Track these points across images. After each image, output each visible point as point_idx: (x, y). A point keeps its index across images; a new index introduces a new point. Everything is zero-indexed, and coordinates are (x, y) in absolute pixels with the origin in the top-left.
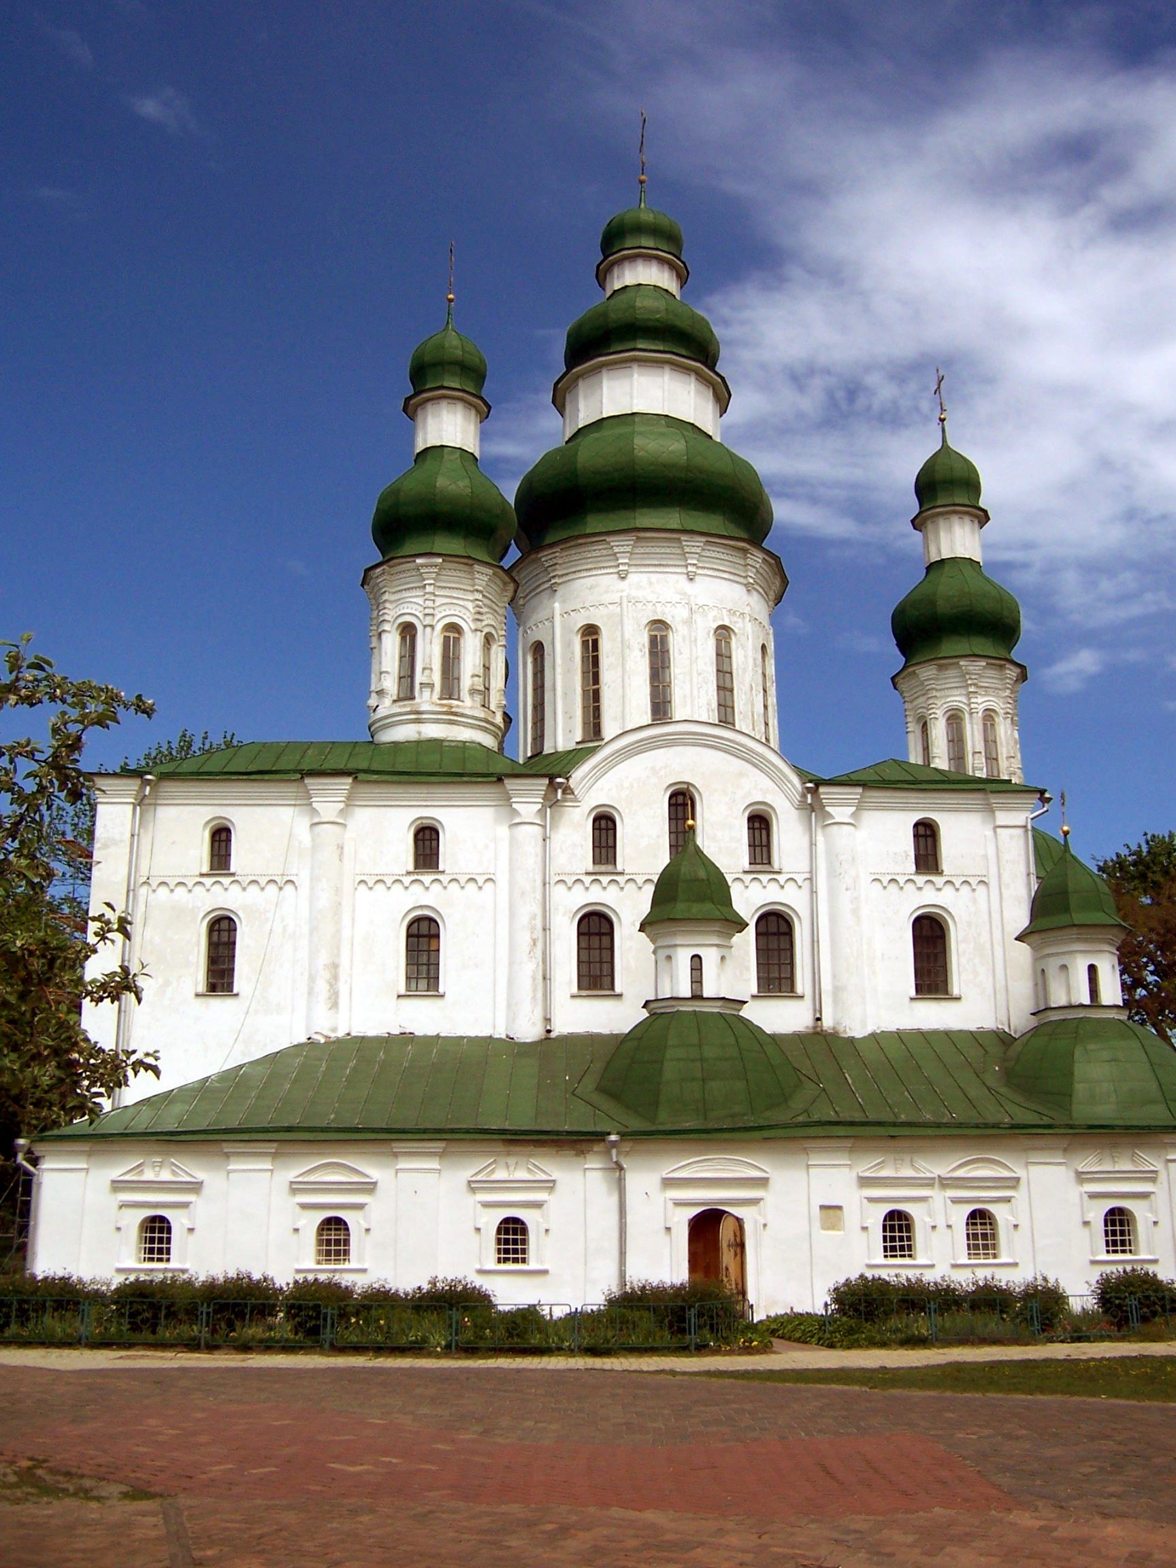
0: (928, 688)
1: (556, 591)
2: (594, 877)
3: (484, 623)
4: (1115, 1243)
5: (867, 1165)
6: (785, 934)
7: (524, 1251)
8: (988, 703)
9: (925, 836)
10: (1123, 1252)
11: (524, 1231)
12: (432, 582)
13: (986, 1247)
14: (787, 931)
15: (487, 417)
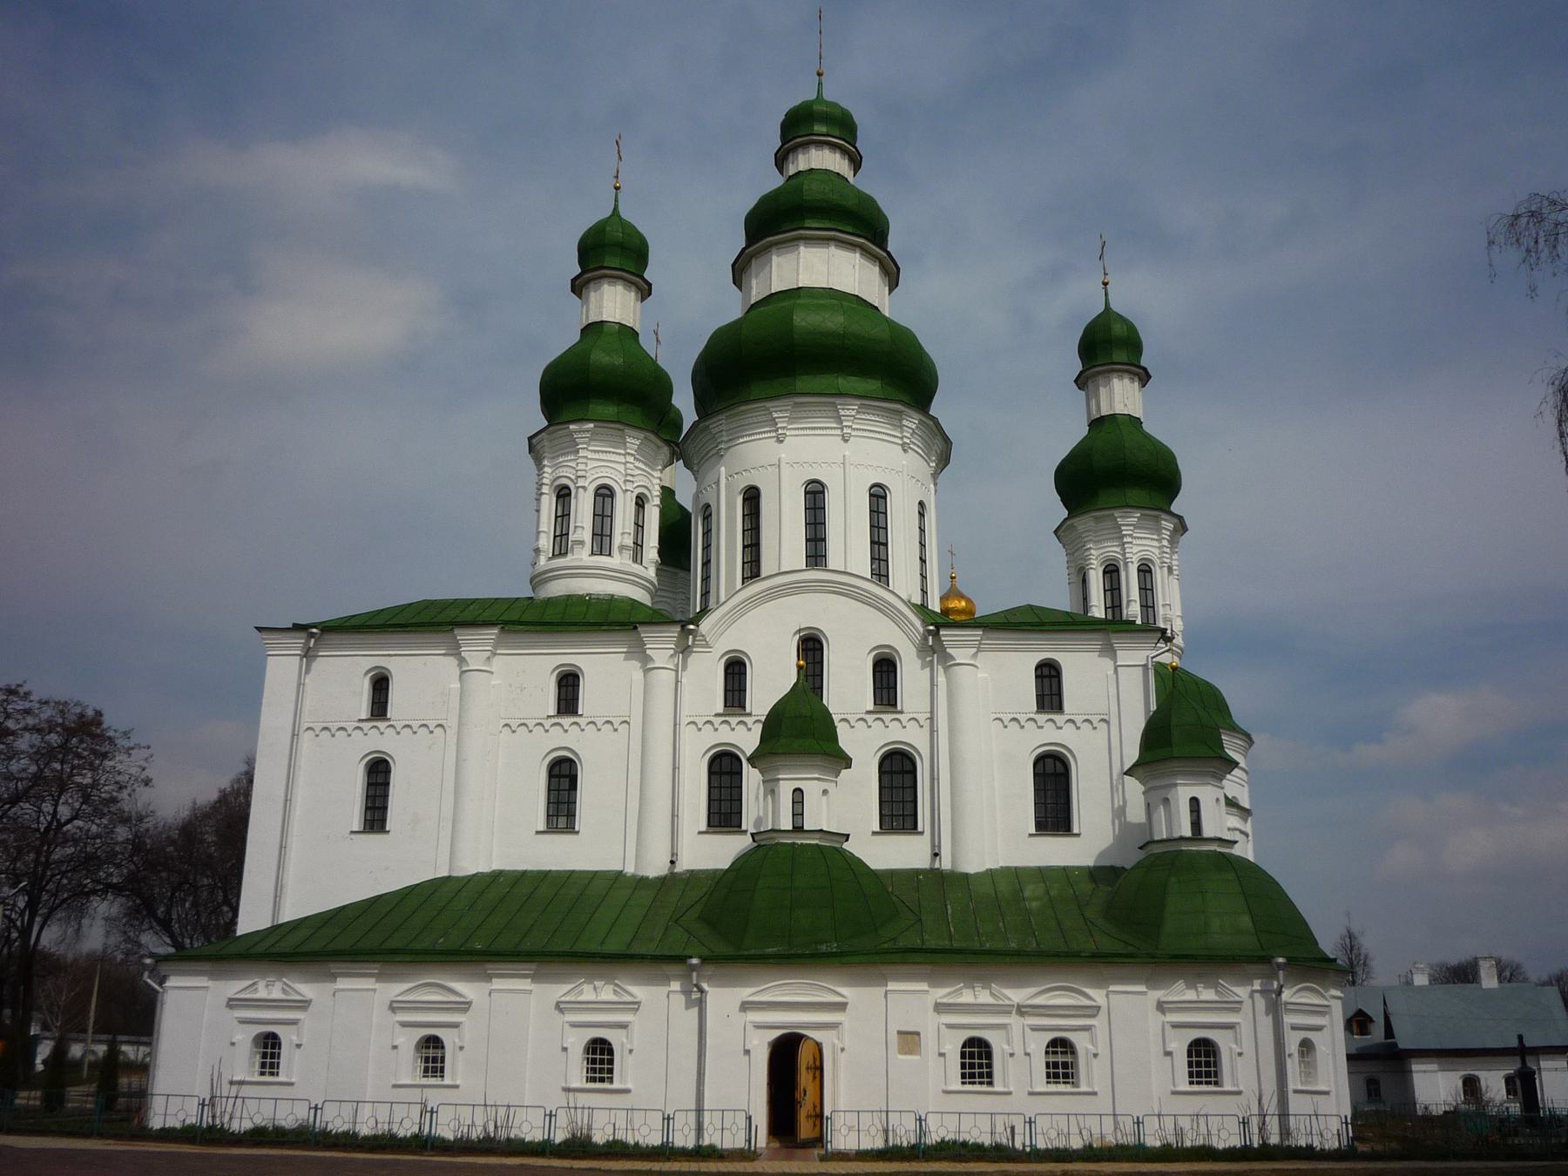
0: (1086, 539)
1: (722, 455)
2: (724, 719)
3: (636, 485)
4: (1199, 1074)
5: (941, 993)
6: (908, 772)
7: (611, 1071)
8: (1141, 554)
9: (1050, 677)
10: (1208, 1083)
11: (611, 1052)
12: (585, 446)
13: (1066, 1076)
14: (911, 769)
15: (650, 294)
